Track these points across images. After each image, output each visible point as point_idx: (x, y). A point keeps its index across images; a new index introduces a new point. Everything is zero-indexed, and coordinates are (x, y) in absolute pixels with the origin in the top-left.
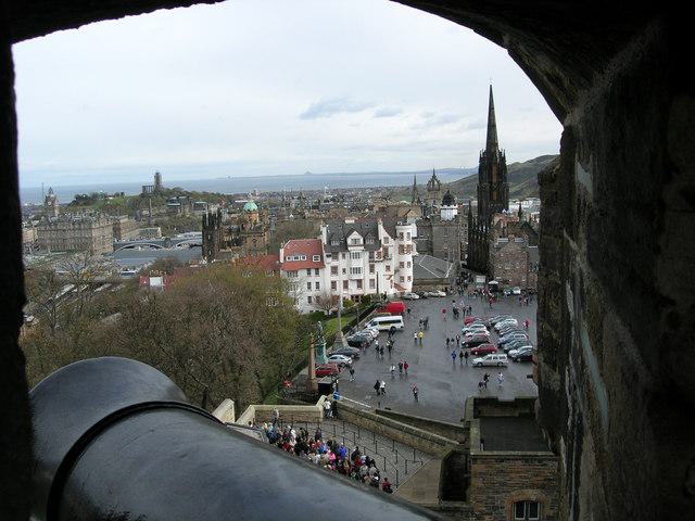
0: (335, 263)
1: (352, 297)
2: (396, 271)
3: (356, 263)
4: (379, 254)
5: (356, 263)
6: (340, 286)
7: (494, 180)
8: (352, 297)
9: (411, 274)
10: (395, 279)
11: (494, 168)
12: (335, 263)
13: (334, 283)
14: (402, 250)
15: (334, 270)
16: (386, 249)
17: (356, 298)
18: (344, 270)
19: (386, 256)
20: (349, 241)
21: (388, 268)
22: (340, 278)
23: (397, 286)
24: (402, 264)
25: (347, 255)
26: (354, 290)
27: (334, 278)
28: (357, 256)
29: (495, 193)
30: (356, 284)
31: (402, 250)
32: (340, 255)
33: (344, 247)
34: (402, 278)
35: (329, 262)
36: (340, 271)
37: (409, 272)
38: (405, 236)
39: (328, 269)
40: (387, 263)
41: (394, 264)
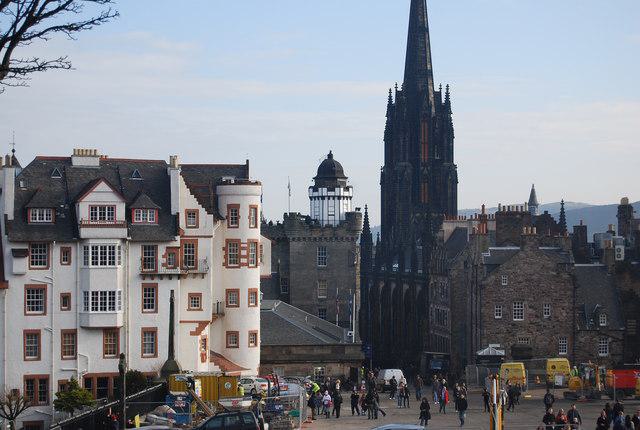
0: (37, 276)
1: (88, 380)
2: (219, 314)
3: (101, 279)
4: (171, 251)
5: (101, 279)
6: (51, 345)
7: (423, 157)
9: (256, 326)
10: (217, 344)
11: (424, 127)
12: (37, 276)
13: (32, 340)
14: (233, 254)
15: (36, 298)
16: (190, 246)
17: (99, 384)
18: (66, 300)
19: (188, 262)
21: (195, 300)
22: (54, 322)
23: (217, 358)
24: (232, 296)
25: (76, 252)
26: (93, 359)
27: (35, 322)
28: (106, 256)
29: (424, 187)
30: (98, 341)
31: (233, 254)
32: (56, 253)
33: (68, 229)
34: (233, 338)
36: (53, 299)
37: (251, 319)
38: (244, 213)
39: (16, 292)
41: (211, 289)
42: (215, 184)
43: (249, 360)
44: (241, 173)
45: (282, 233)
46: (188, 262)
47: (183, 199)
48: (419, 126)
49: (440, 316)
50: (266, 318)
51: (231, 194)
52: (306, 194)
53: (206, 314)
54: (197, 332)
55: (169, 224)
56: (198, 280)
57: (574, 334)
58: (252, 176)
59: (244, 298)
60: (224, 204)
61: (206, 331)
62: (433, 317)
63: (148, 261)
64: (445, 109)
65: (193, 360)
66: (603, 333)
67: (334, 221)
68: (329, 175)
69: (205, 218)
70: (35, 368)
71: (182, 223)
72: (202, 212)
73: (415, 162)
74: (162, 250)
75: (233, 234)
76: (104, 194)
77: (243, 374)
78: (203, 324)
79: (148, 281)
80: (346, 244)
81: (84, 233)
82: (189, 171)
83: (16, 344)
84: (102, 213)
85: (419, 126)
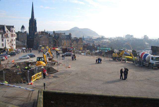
2: (11, 42)
4: (5, 35)
9: (15, 43)
14: (12, 35)
21: (8, 40)
23: (11, 47)
24: (12, 40)
31: (12, 35)
34: (12, 45)
37: (14, 43)
38: (13, 31)
40: (7, 39)
42: (10, 28)
43: (14, 47)
44: (13, 27)
45: (18, 33)
46: (7, 36)
47: (6, 29)
48: (33, 23)
49: (35, 42)
50: (16, 42)
51: (12, 29)
52: (20, 29)
53: (9, 42)
54: (8, 44)
55: (5, 32)
58: (14, 27)
59: (14, 40)
61: (9, 44)
62: (34, 42)
64: (36, 21)
65: (8, 47)
66: (52, 44)
67: (24, 32)
68: (23, 27)
69: (9, 31)
71: (6, 32)
72: (9, 31)
74: (4, 35)
75: (12, 33)
77: (14, 48)
78: (9, 43)
79: (2, 38)
80: (25, 35)
82: (7, 26)
85: (33, 23)
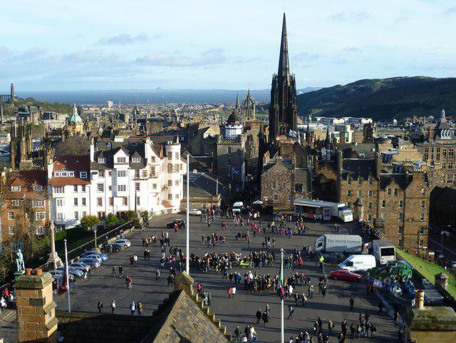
0: (101, 180)
3: (120, 181)
5: (120, 181)
8: (118, 213)
12: (101, 180)
15: (101, 187)
16: (153, 169)
20: (115, 161)
21: (155, 186)
26: (120, 207)
27: (101, 194)
28: (123, 174)
31: (170, 168)
32: (107, 172)
33: (110, 164)
35: (96, 179)
37: (177, 190)
38: (174, 155)
55: (145, 162)
56: (155, 179)
57: (293, 193)
59: (174, 183)
60: (167, 151)
61: (159, 196)
63: (138, 175)
69: (157, 158)
70: (102, 209)
71: (149, 161)
73: (280, 105)
74: (141, 171)
76: (121, 154)
78: (157, 193)
81: (115, 167)
83: (94, 202)
84: (121, 161)
